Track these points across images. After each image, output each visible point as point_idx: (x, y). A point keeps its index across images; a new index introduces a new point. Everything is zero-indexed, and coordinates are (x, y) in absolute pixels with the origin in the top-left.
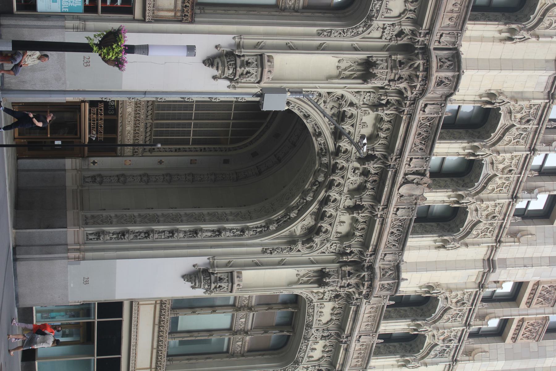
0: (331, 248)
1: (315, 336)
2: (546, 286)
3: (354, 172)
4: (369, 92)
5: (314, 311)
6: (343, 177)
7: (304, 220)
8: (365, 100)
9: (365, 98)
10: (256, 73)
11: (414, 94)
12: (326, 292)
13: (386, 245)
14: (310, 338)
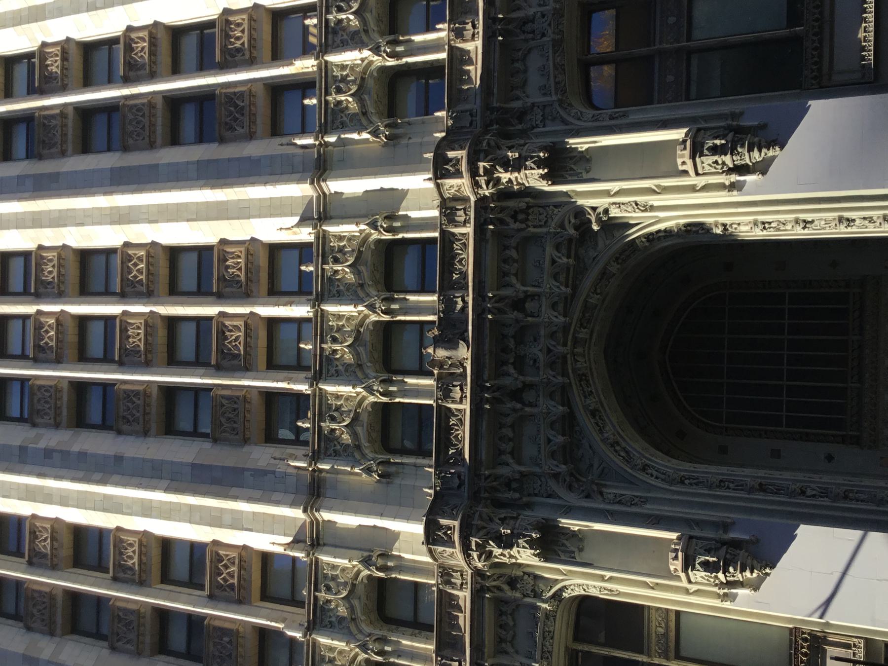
0: (546, 217)
1: (544, 20)
2: (240, 130)
3: (535, 361)
4: (536, 495)
5: (555, 77)
6: (549, 351)
7: (594, 259)
8: (540, 483)
9: (540, 486)
10: (695, 549)
11: (477, 516)
12: (541, 122)
13: (468, 240)
14: (553, 14)
